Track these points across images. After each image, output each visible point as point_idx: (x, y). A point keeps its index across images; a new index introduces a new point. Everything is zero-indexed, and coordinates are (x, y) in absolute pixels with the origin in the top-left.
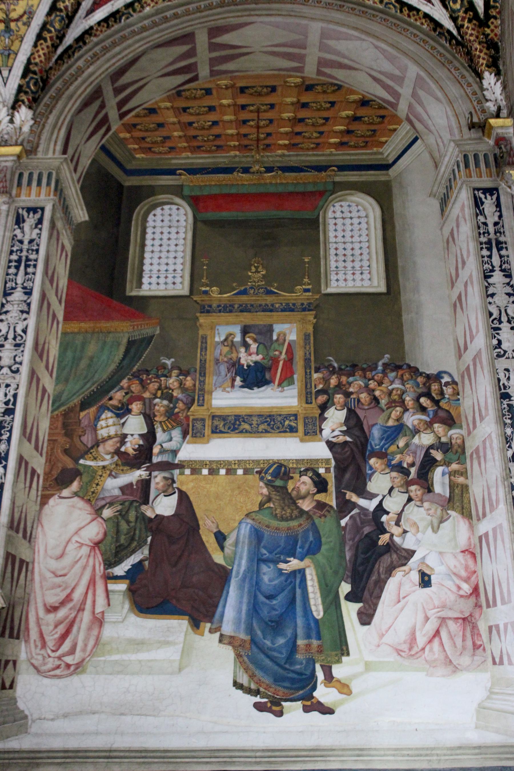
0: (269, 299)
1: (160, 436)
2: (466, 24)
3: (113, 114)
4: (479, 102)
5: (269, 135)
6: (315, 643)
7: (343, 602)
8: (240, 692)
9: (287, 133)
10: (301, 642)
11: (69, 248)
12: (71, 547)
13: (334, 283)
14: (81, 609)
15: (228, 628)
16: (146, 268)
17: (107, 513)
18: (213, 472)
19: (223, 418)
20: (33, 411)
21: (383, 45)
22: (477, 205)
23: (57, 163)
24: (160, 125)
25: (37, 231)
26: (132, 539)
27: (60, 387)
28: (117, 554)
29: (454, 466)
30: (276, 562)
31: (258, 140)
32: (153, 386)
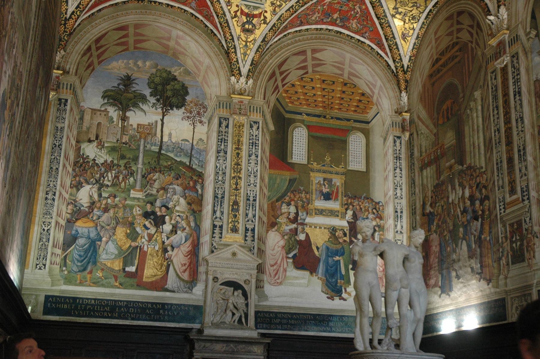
0: (331, 169)
1: (300, 214)
2: (400, 72)
3: (280, 85)
4: (399, 100)
5: (332, 103)
6: (342, 281)
7: (350, 270)
8: (323, 294)
9: (338, 103)
10: (339, 281)
11: (269, 140)
12: (276, 247)
13: (351, 166)
14: (280, 266)
15: (320, 276)
16: (294, 152)
17: (286, 237)
18: (315, 227)
19: (318, 210)
20: (262, 201)
21: (370, 69)
22: (394, 143)
23: (262, 103)
24: (296, 92)
25: (257, 132)
26: (293, 246)
27: (270, 193)
28: (289, 251)
29: (381, 233)
30: (333, 257)
31: (328, 105)
32: (297, 196)
